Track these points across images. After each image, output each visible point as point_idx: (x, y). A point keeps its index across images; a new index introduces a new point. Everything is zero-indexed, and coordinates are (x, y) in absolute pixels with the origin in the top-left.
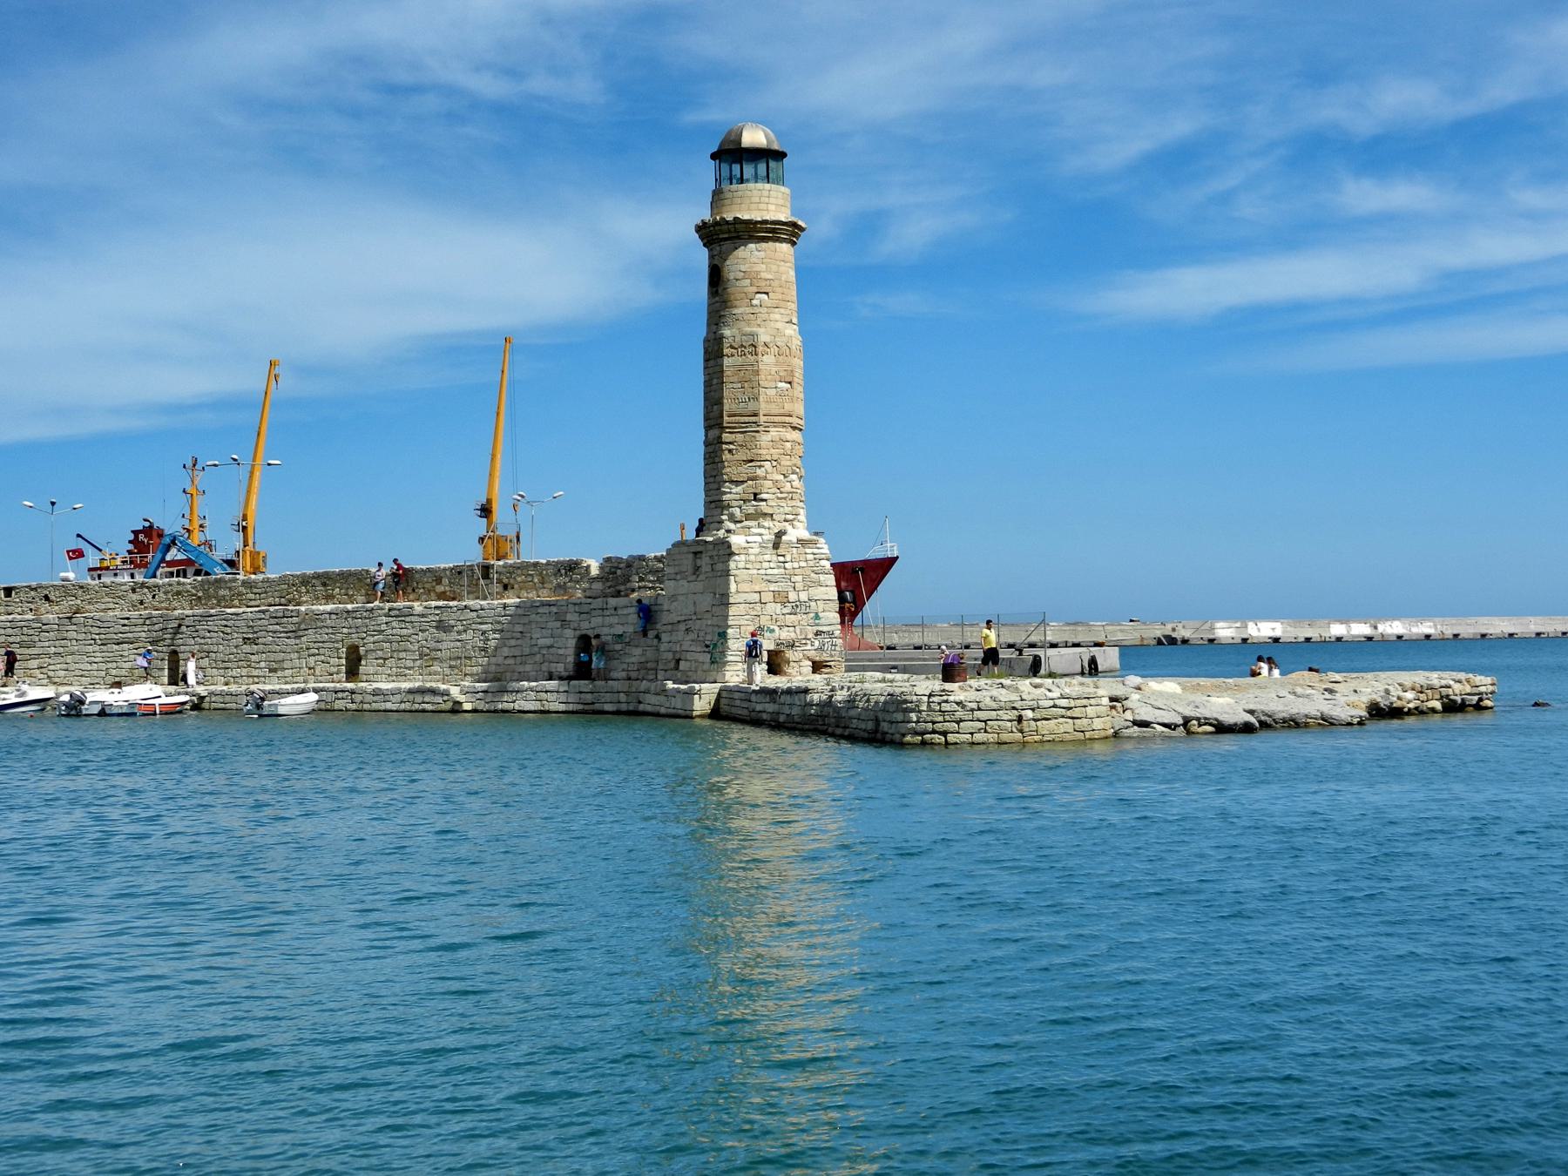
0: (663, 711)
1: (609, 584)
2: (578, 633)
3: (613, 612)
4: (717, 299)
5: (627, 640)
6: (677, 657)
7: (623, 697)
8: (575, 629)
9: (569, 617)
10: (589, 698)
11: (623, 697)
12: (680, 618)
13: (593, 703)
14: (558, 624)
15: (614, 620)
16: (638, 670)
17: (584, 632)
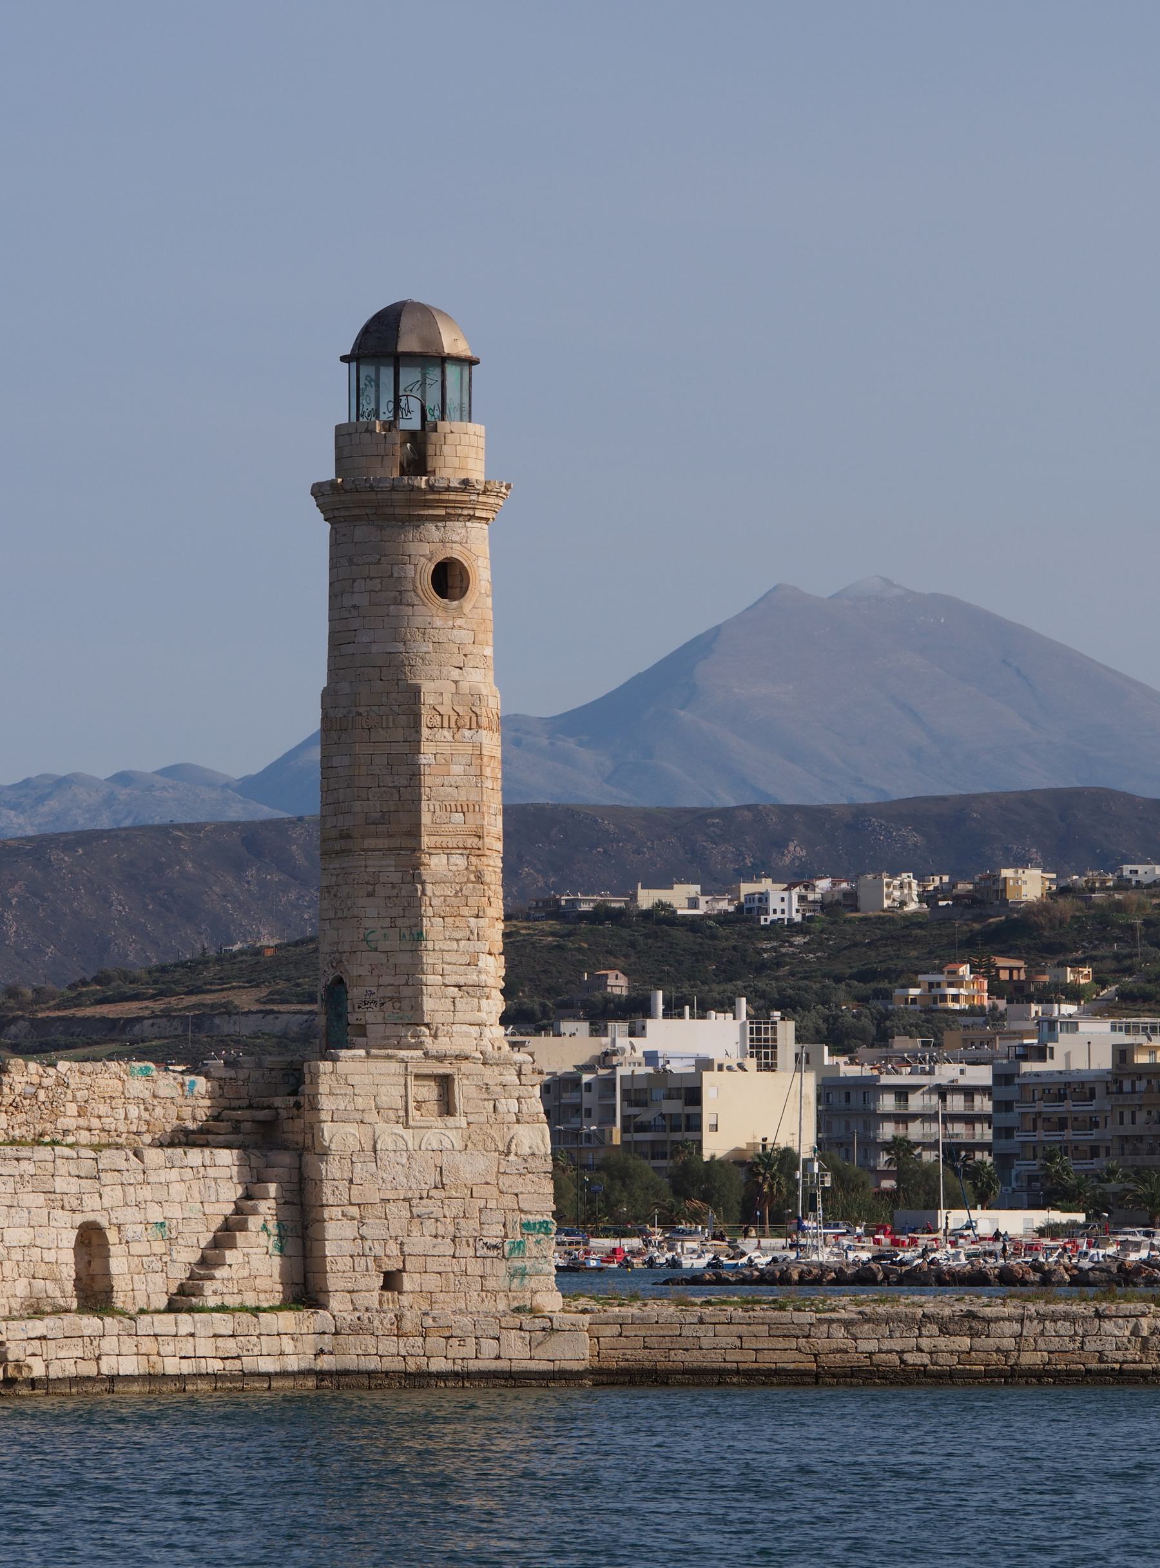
0: (438, 1365)
1: (21, 1117)
2: (79, 1219)
3: (140, 1177)
4: (459, 622)
5: (174, 1235)
6: (392, 1265)
7: (288, 1345)
8: (73, 1211)
9: (60, 1185)
10: (230, 1346)
11: (288, 1345)
12: (390, 1195)
13: (238, 1357)
14: (40, 1199)
15: (145, 1193)
16: (240, 1292)
17: (91, 1217)
